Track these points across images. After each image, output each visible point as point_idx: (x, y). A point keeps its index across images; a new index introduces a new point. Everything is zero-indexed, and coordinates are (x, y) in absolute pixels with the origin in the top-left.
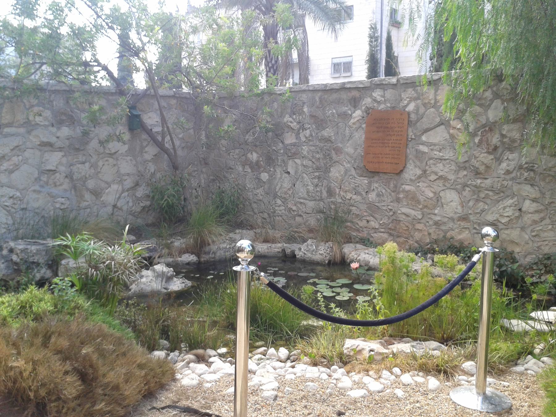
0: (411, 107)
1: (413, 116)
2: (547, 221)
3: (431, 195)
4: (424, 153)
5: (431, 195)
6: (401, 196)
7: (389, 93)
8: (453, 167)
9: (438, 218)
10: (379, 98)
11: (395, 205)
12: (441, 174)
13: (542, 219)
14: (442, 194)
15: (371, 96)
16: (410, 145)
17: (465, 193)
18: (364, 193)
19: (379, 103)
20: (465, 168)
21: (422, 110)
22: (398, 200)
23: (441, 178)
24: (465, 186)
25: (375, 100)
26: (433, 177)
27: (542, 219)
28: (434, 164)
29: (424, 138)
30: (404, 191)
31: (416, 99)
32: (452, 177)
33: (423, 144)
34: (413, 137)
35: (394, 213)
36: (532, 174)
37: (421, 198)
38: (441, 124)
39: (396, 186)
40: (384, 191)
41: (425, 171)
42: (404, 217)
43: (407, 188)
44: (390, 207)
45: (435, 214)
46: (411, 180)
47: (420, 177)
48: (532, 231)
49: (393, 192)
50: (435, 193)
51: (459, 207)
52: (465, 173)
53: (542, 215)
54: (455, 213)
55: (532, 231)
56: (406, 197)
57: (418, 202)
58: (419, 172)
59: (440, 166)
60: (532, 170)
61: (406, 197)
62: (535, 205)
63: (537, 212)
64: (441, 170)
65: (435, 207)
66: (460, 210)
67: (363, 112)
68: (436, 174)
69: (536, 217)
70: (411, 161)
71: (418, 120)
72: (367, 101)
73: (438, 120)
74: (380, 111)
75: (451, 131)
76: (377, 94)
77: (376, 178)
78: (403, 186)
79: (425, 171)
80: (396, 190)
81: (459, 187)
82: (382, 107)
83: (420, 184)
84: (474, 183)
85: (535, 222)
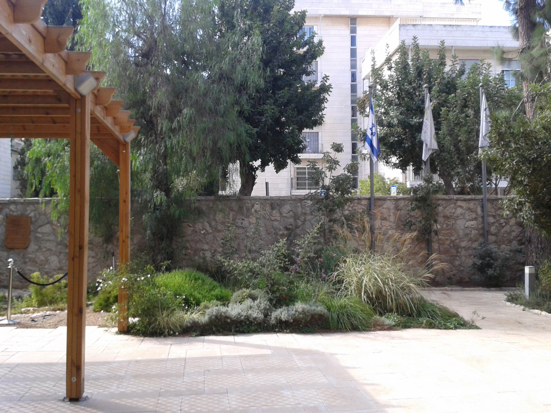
0: (32, 214)
1: (33, 219)
2: (99, 266)
3: (43, 259)
4: (39, 238)
5: (43, 259)
6: (27, 260)
7: (19, 207)
8: (55, 244)
9: (46, 270)
10: (13, 209)
11: (24, 265)
12: (48, 247)
13: (97, 265)
14: (49, 258)
15: (9, 208)
16: (32, 233)
17: (61, 257)
18: (5, 261)
19: (13, 211)
20: (61, 245)
21: (38, 216)
22: (25, 263)
23: (48, 250)
24: (60, 253)
25: (11, 210)
26: (44, 250)
27: (97, 265)
28: (45, 243)
29: (39, 230)
30: (28, 258)
31: (34, 211)
32: (54, 249)
33: (39, 233)
34: (33, 229)
35: (23, 270)
36: (92, 245)
37: (39, 261)
38: (48, 223)
39: (24, 255)
40: (17, 259)
41: (40, 247)
42: (29, 271)
43: (30, 256)
44: (20, 267)
45: (45, 268)
46: (32, 252)
47: (37, 250)
48: (92, 271)
49: (23, 258)
50: (46, 258)
51: (58, 263)
52: (61, 247)
53: (97, 263)
54: (56, 267)
55: (92, 271)
56: (30, 261)
57: (36, 262)
58: (37, 247)
59: (48, 244)
60: (91, 244)
61: (30, 261)
62: (93, 259)
63: (94, 262)
64: (48, 245)
65: (45, 265)
66: (58, 265)
67: (4, 216)
68: (46, 248)
69: (94, 265)
70: (32, 242)
71: (36, 221)
72: (6, 210)
73: (46, 221)
74: (15, 216)
75: (54, 227)
76: (12, 207)
77: (12, 252)
78: (28, 255)
79: (40, 247)
80: (24, 257)
81: (58, 254)
82: (15, 214)
83: (38, 254)
84: (65, 251)
85: (94, 267)
